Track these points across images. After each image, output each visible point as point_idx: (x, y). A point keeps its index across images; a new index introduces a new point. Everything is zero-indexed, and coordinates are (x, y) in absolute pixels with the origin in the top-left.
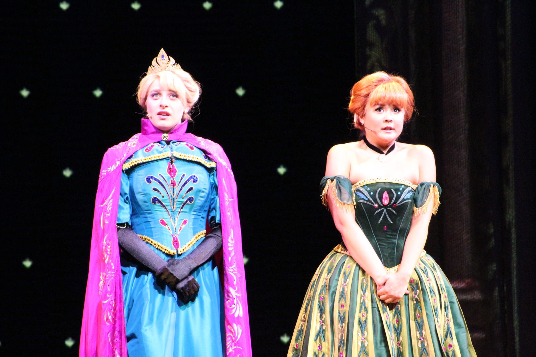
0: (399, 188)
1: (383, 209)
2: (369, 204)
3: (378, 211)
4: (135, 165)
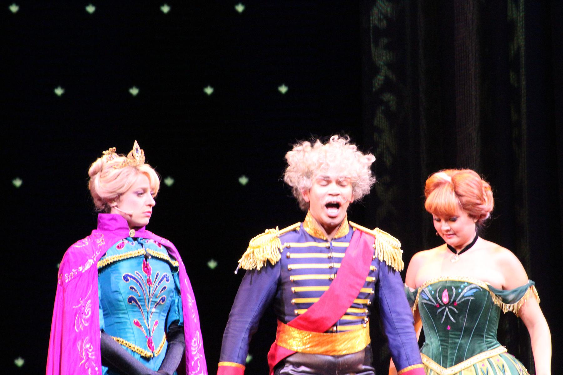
0: (461, 286)
1: (444, 307)
2: (430, 303)
3: (440, 310)
4: (111, 263)
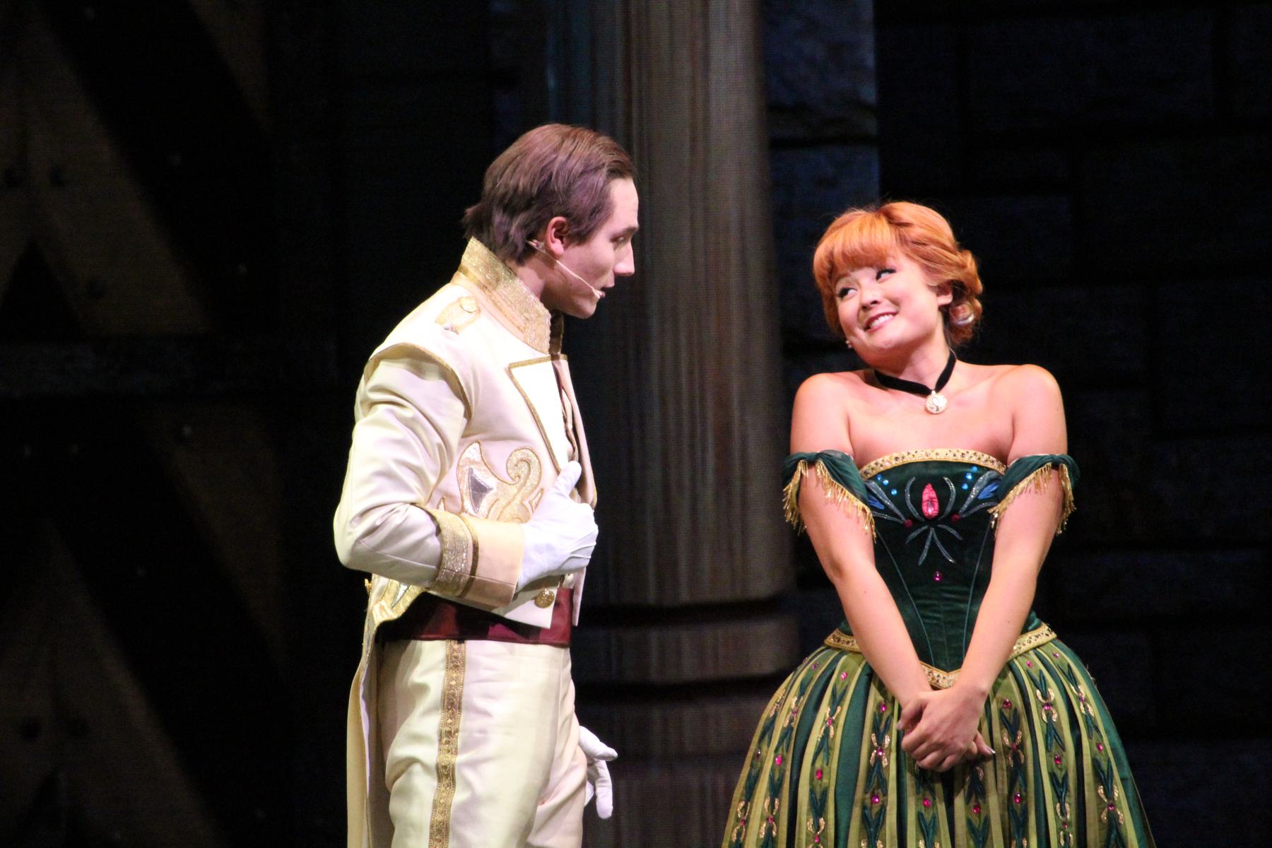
3: (914, 534)
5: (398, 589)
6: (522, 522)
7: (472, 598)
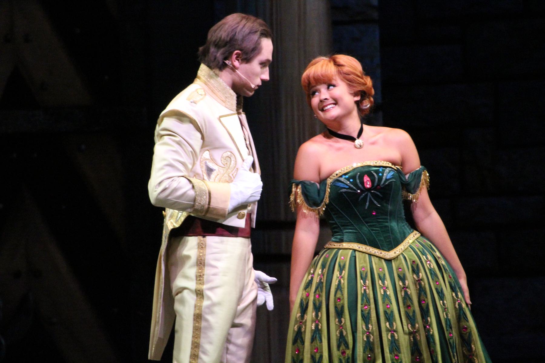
1: (366, 193)
3: (362, 197)
5: (178, 214)
6: (229, 183)
7: (209, 216)
